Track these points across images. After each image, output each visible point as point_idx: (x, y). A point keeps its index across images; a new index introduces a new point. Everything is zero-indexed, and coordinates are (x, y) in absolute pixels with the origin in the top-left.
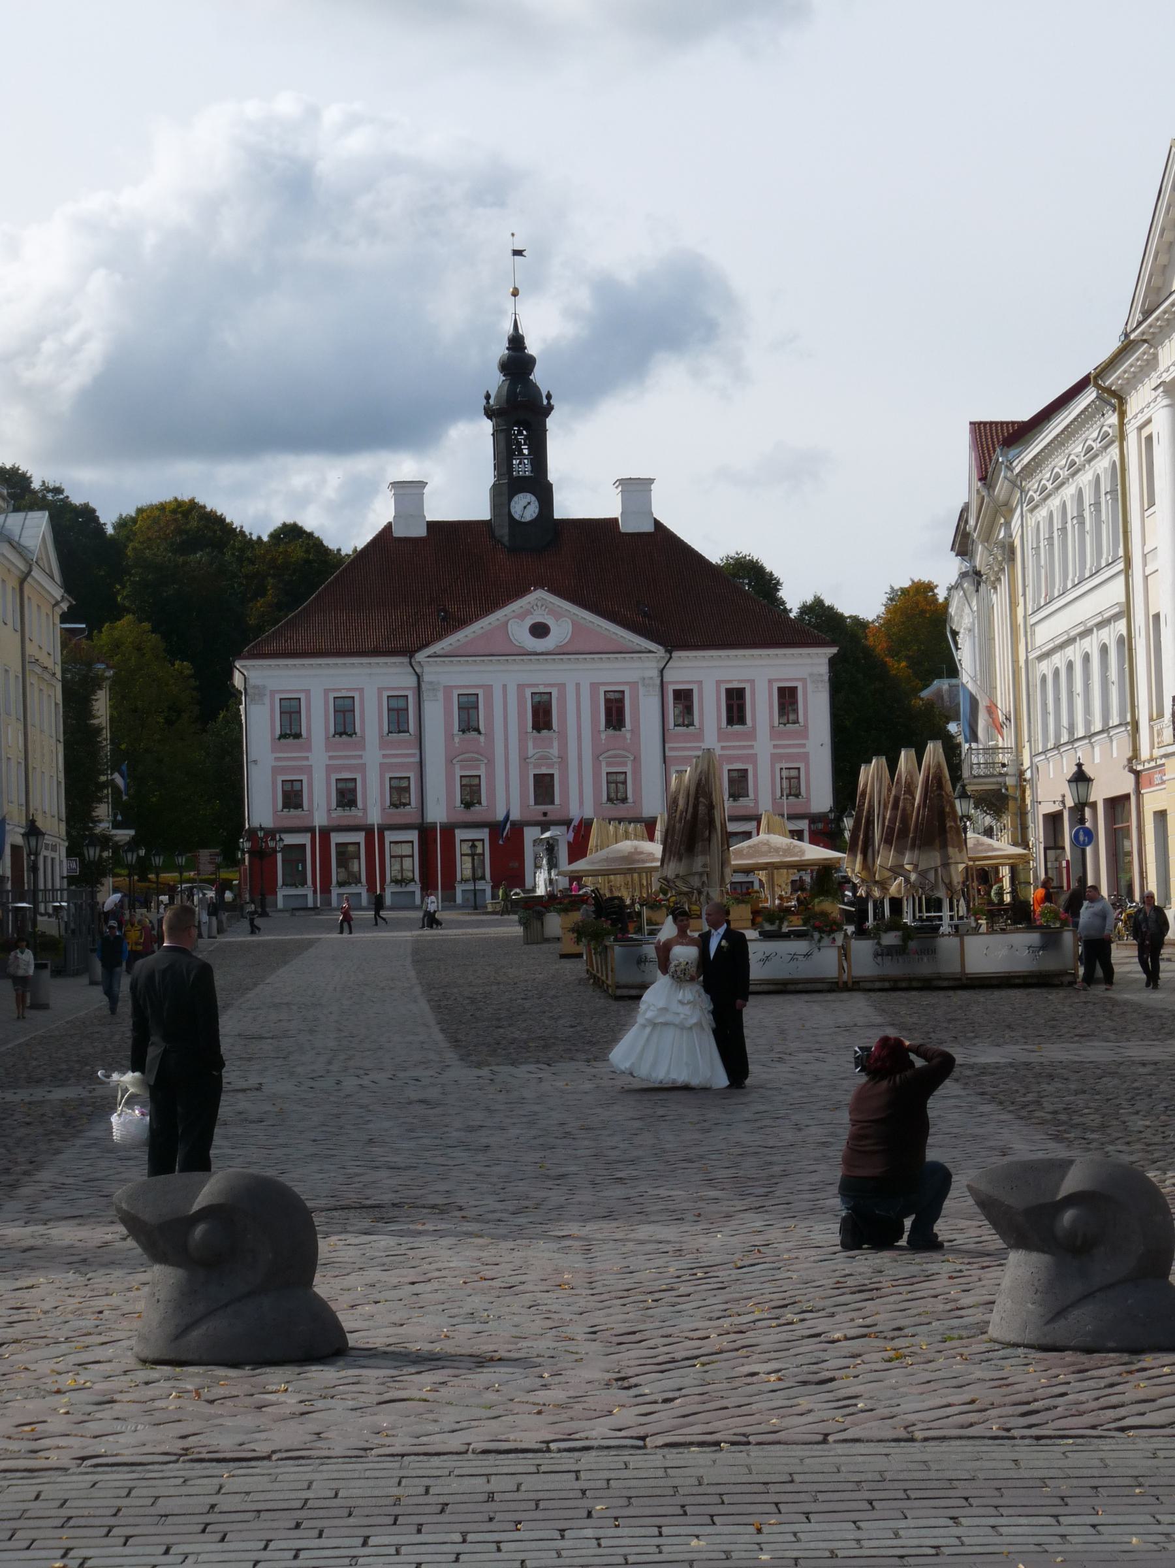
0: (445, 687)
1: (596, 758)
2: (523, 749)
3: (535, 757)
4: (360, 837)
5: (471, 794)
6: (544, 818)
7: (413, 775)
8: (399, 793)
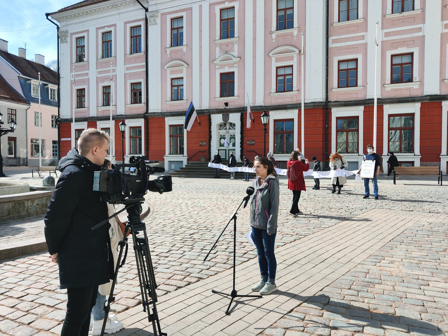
0: (162, 14)
1: (267, 55)
3: (220, 59)
6: (226, 107)
7: (143, 81)
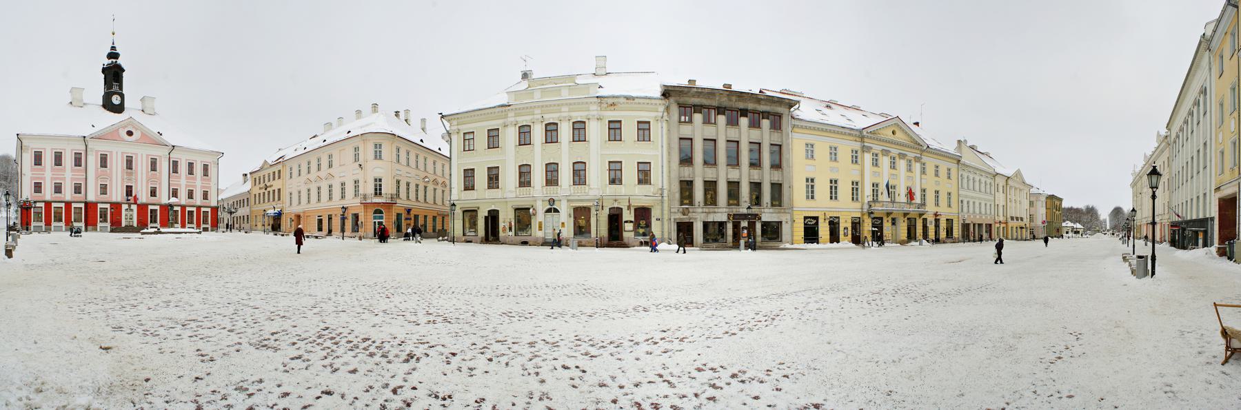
2: (122, 177)
4: (63, 205)
5: (104, 189)
8: (77, 189)
